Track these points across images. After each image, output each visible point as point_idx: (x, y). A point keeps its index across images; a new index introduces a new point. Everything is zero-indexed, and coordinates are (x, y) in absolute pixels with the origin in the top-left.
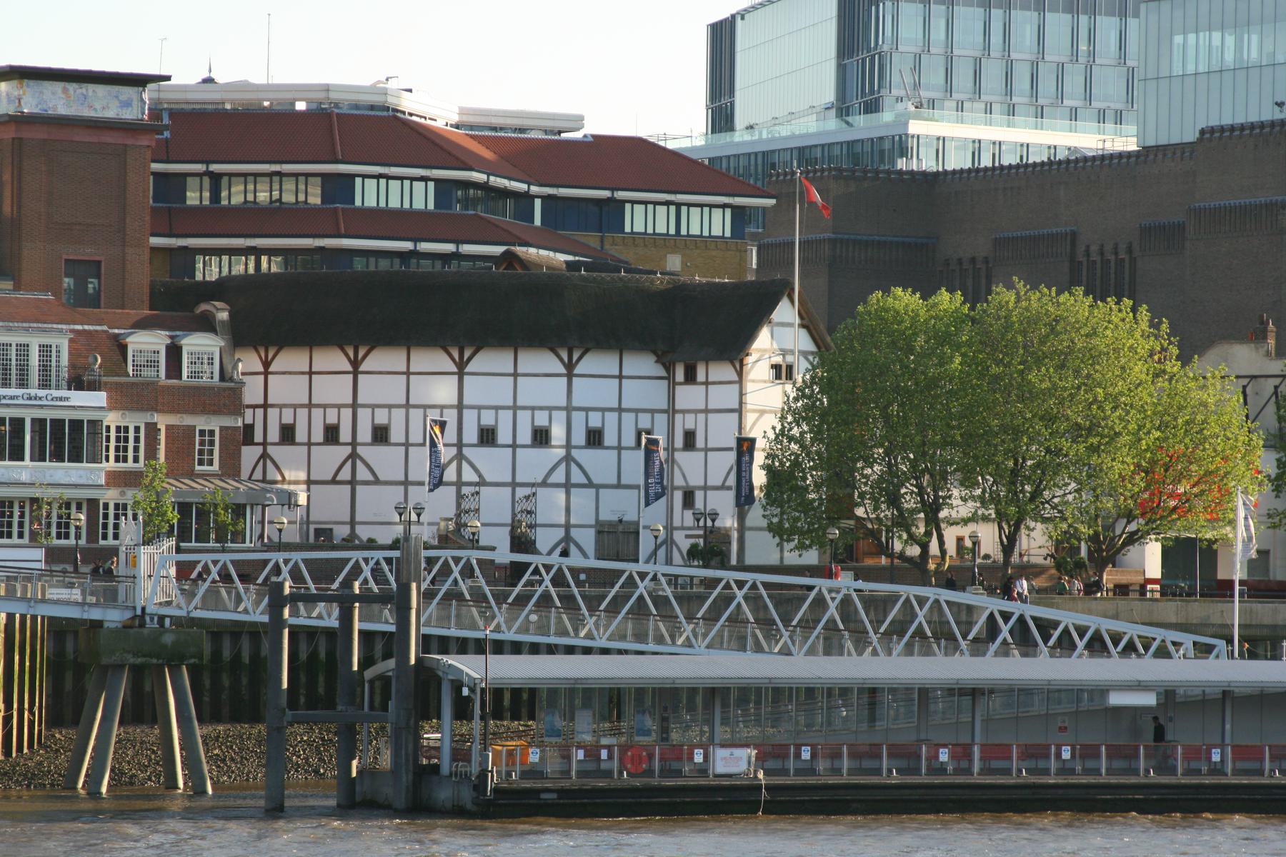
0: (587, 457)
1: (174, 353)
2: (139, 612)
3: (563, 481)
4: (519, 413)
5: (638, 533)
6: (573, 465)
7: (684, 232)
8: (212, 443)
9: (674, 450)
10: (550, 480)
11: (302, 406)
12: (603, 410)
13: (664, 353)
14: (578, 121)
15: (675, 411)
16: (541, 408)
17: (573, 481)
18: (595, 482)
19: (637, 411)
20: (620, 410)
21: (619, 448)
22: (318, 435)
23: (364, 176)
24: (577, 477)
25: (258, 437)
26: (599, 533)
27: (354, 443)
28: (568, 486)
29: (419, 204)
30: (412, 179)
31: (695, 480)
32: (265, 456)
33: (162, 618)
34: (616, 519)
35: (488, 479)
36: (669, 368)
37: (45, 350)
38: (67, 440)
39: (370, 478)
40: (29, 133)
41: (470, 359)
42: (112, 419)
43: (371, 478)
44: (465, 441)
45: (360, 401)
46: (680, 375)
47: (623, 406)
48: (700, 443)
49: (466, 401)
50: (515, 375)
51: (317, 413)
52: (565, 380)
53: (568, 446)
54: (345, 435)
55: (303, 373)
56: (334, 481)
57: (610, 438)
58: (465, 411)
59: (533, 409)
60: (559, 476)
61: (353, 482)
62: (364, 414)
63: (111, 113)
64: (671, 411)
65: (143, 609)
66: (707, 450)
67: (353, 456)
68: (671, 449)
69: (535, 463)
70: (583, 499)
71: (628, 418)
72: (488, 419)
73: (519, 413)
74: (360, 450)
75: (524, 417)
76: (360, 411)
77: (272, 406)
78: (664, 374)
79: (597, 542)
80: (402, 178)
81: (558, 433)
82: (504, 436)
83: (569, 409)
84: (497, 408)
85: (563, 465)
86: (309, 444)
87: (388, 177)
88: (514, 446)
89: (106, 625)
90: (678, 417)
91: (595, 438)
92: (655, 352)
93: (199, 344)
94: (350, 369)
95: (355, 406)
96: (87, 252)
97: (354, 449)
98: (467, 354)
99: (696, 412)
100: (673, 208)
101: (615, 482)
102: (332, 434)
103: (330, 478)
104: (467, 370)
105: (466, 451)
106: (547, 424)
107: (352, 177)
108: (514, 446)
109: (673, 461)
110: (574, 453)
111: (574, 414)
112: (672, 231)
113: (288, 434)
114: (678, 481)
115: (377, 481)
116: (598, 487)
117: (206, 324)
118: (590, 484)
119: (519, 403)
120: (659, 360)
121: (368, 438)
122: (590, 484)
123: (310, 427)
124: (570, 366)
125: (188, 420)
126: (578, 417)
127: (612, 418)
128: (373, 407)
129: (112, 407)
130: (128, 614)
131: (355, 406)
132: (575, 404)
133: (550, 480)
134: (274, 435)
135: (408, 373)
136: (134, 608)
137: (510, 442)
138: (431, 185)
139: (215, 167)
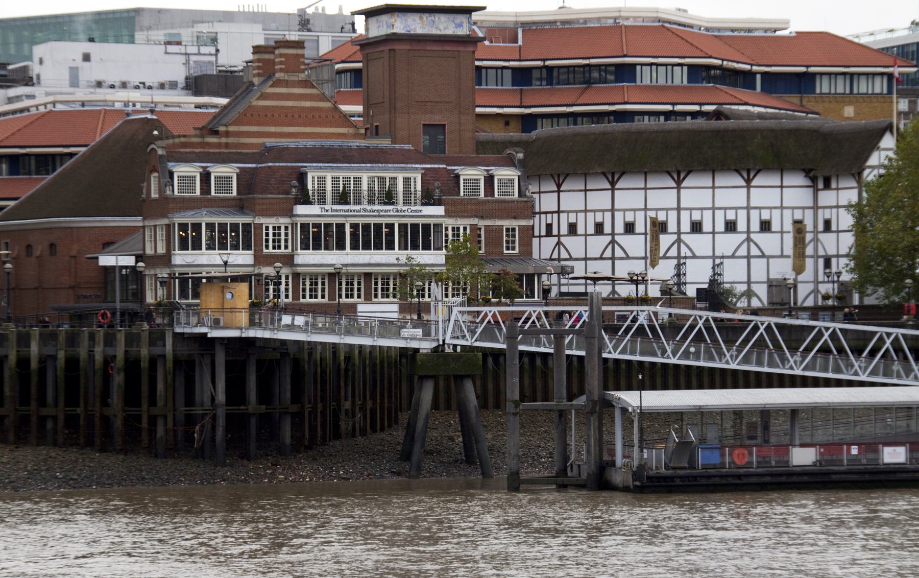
0: (761, 239)
1: (489, 179)
2: (441, 343)
3: (746, 254)
4: (717, 212)
5: (795, 287)
6: (752, 244)
7: (855, 91)
8: (514, 236)
9: (818, 232)
10: (737, 254)
11: (581, 211)
13: (811, 170)
14: (785, 25)
15: (818, 208)
16: (731, 208)
17: (752, 254)
18: (767, 253)
19: (793, 208)
20: (782, 208)
22: (591, 230)
23: (642, 65)
24: (754, 251)
25: (555, 232)
26: (770, 286)
27: (613, 234)
28: (749, 257)
29: (677, 81)
30: (673, 65)
31: (832, 251)
32: (559, 243)
33: (455, 346)
34: (780, 277)
35: (697, 255)
36: (814, 180)
37: (407, 181)
38: (419, 236)
39: (624, 256)
40: (398, 47)
41: (684, 179)
42: (450, 222)
43: (624, 256)
45: (616, 207)
46: (821, 185)
47: (784, 205)
48: (834, 228)
49: (682, 206)
50: (713, 187)
51: (590, 216)
52: (745, 190)
53: (748, 232)
54: (607, 229)
55: (581, 191)
56: (601, 258)
57: (775, 226)
58: (682, 212)
59: (725, 209)
60: (743, 251)
61: (613, 259)
63: (450, 32)
64: (815, 207)
65: (444, 341)
66: (838, 232)
67: (613, 242)
68: (815, 231)
69: (727, 243)
70: (758, 266)
71: (787, 213)
72: (696, 216)
73: (717, 212)
74: (617, 238)
75: (720, 215)
76: (616, 213)
77: (563, 212)
78: (810, 184)
79: (768, 292)
80: (666, 65)
81: (742, 226)
82: (707, 227)
83: (748, 208)
84: (702, 209)
85: (746, 244)
86: (586, 235)
87: (657, 65)
88: (713, 233)
89: (421, 351)
90: (820, 211)
91: (765, 226)
92: (804, 170)
93: (506, 174)
94: (609, 187)
95: (613, 210)
96: (437, 119)
97: (613, 238)
98: (682, 177)
99: (831, 207)
100: (848, 77)
101: (779, 253)
102: (599, 229)
103: (599, 256)
105: (683, 237)
106: (733, 218)
107: (634, 66)
108: (713, 233)
109: (818, 240)
110: (752, 236)
111: (752, 212)
112: (848, 91)
113: (573, 229)
114: (821, 252)
115: (628, 257)
116: (769, 257)
117: (509, 162)
118: (763, 256)
119: (716, 206)
121: (622, 231)
122: (763, 256)
123: (586, 224)
124: (748, 181)
125: (499, 223)
126: (754, 214)
127: (776, 214)
128: (624, 210)
129: (448, 214)
130: (434, 344)
131: (613, 210)
132: (752, 204)
133: (737, 254)
134: (564, 230)
135: (646, 189)
136: (438, 340)
138: (685, 68)
139: (548, 63)
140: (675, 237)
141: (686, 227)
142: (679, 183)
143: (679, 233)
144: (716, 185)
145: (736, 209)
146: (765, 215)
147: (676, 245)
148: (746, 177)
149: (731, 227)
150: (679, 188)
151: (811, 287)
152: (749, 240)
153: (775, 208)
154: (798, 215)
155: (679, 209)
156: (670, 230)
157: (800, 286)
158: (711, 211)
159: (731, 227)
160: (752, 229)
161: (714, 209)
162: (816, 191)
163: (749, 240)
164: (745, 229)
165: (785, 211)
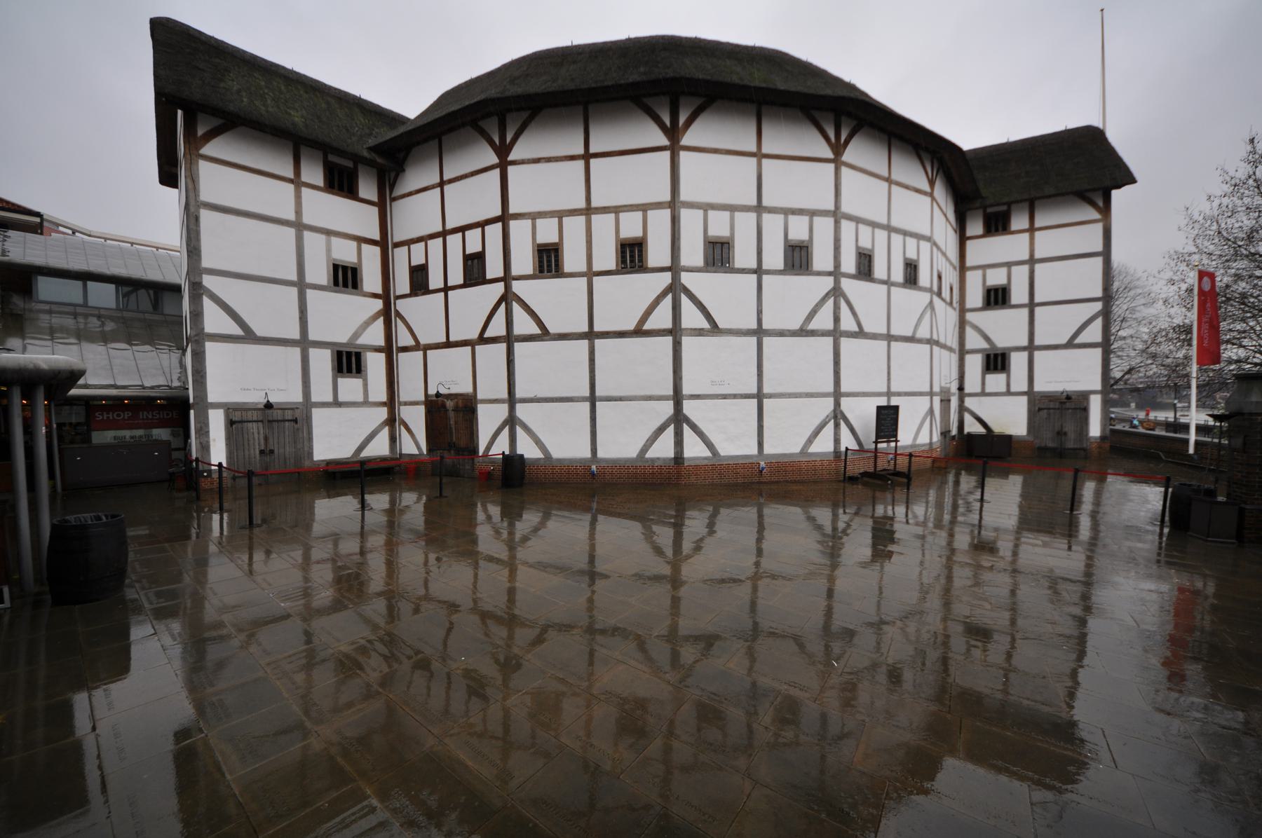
12: (732, 209)
20: (759, 208)
21: (759, 271)
24: (691, 317)
28: (675, 332)
44: (515, 271)
49: (512, 210)
52: (666, 155)
57: (743, 255)
60: (661, 318)
71: (773, 223)
72: (547, 233)
81: (658, 254)
85: (670, 296)
91: (719, 254)
104: (511, 157)
105: (517, 287)
110: (686, 278)
119: (594, 204)
124: (673, 133)
126: (691, 221)
127: (746, 222)
137: (584, 268)
140: (499, 288)
141: (523, 261)
142: (503, 151)
143: (507, 278)
144: (592, 150)
145: (644, 208)
146: (719, 226)
148: (667, 121)
149: (632, 255)
150: (503, 166)
152: (675, 290)
154: (798, 231)
155: (504, 218)
156: (490, 275)
158: (582, 219)
159: (632, 255)
160: (685, 261)
161: (588, 211)
163: (675, 290)
164: (667, 262)
165: (766, 217)
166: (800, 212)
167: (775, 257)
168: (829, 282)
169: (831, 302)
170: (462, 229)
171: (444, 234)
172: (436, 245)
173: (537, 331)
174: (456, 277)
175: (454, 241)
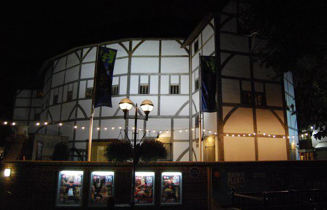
9: (192, 94)
57: (153, 90)
62: (52, 91)
68: (190, 95)
78: (187, 54)
90: (193, 75)
92: (180, 43)
105: (80, 102)
106: (118, 84)
109: (192, 101)
111: (132, 77)
120: (183, 45)
127: (154, 79)
140: (75, 103)
146: (144, 81)
147: (75, 110)
151: (186, 145)
153: (154, 74)
157: (175, 144)
162: (190, 57)
166: (174, 74)
167: (165, 89)
168: (187, 98)
169: (188, 106)
170: (68, 84)
171: (64, 85)
172: (61, 88)
173: (84, 117)
174: (65, 99)
175: (66, 87)
